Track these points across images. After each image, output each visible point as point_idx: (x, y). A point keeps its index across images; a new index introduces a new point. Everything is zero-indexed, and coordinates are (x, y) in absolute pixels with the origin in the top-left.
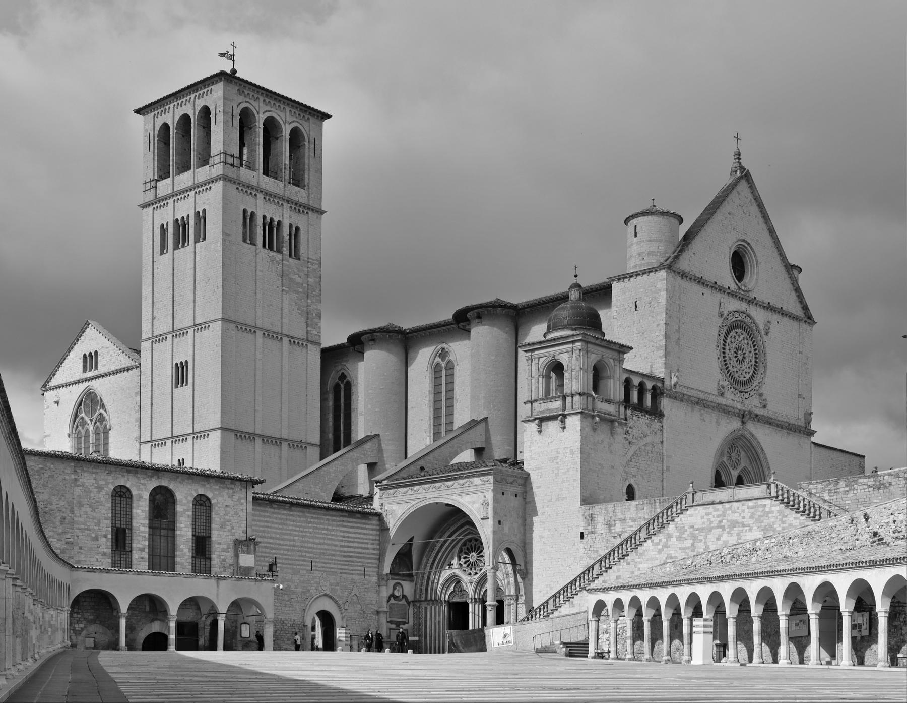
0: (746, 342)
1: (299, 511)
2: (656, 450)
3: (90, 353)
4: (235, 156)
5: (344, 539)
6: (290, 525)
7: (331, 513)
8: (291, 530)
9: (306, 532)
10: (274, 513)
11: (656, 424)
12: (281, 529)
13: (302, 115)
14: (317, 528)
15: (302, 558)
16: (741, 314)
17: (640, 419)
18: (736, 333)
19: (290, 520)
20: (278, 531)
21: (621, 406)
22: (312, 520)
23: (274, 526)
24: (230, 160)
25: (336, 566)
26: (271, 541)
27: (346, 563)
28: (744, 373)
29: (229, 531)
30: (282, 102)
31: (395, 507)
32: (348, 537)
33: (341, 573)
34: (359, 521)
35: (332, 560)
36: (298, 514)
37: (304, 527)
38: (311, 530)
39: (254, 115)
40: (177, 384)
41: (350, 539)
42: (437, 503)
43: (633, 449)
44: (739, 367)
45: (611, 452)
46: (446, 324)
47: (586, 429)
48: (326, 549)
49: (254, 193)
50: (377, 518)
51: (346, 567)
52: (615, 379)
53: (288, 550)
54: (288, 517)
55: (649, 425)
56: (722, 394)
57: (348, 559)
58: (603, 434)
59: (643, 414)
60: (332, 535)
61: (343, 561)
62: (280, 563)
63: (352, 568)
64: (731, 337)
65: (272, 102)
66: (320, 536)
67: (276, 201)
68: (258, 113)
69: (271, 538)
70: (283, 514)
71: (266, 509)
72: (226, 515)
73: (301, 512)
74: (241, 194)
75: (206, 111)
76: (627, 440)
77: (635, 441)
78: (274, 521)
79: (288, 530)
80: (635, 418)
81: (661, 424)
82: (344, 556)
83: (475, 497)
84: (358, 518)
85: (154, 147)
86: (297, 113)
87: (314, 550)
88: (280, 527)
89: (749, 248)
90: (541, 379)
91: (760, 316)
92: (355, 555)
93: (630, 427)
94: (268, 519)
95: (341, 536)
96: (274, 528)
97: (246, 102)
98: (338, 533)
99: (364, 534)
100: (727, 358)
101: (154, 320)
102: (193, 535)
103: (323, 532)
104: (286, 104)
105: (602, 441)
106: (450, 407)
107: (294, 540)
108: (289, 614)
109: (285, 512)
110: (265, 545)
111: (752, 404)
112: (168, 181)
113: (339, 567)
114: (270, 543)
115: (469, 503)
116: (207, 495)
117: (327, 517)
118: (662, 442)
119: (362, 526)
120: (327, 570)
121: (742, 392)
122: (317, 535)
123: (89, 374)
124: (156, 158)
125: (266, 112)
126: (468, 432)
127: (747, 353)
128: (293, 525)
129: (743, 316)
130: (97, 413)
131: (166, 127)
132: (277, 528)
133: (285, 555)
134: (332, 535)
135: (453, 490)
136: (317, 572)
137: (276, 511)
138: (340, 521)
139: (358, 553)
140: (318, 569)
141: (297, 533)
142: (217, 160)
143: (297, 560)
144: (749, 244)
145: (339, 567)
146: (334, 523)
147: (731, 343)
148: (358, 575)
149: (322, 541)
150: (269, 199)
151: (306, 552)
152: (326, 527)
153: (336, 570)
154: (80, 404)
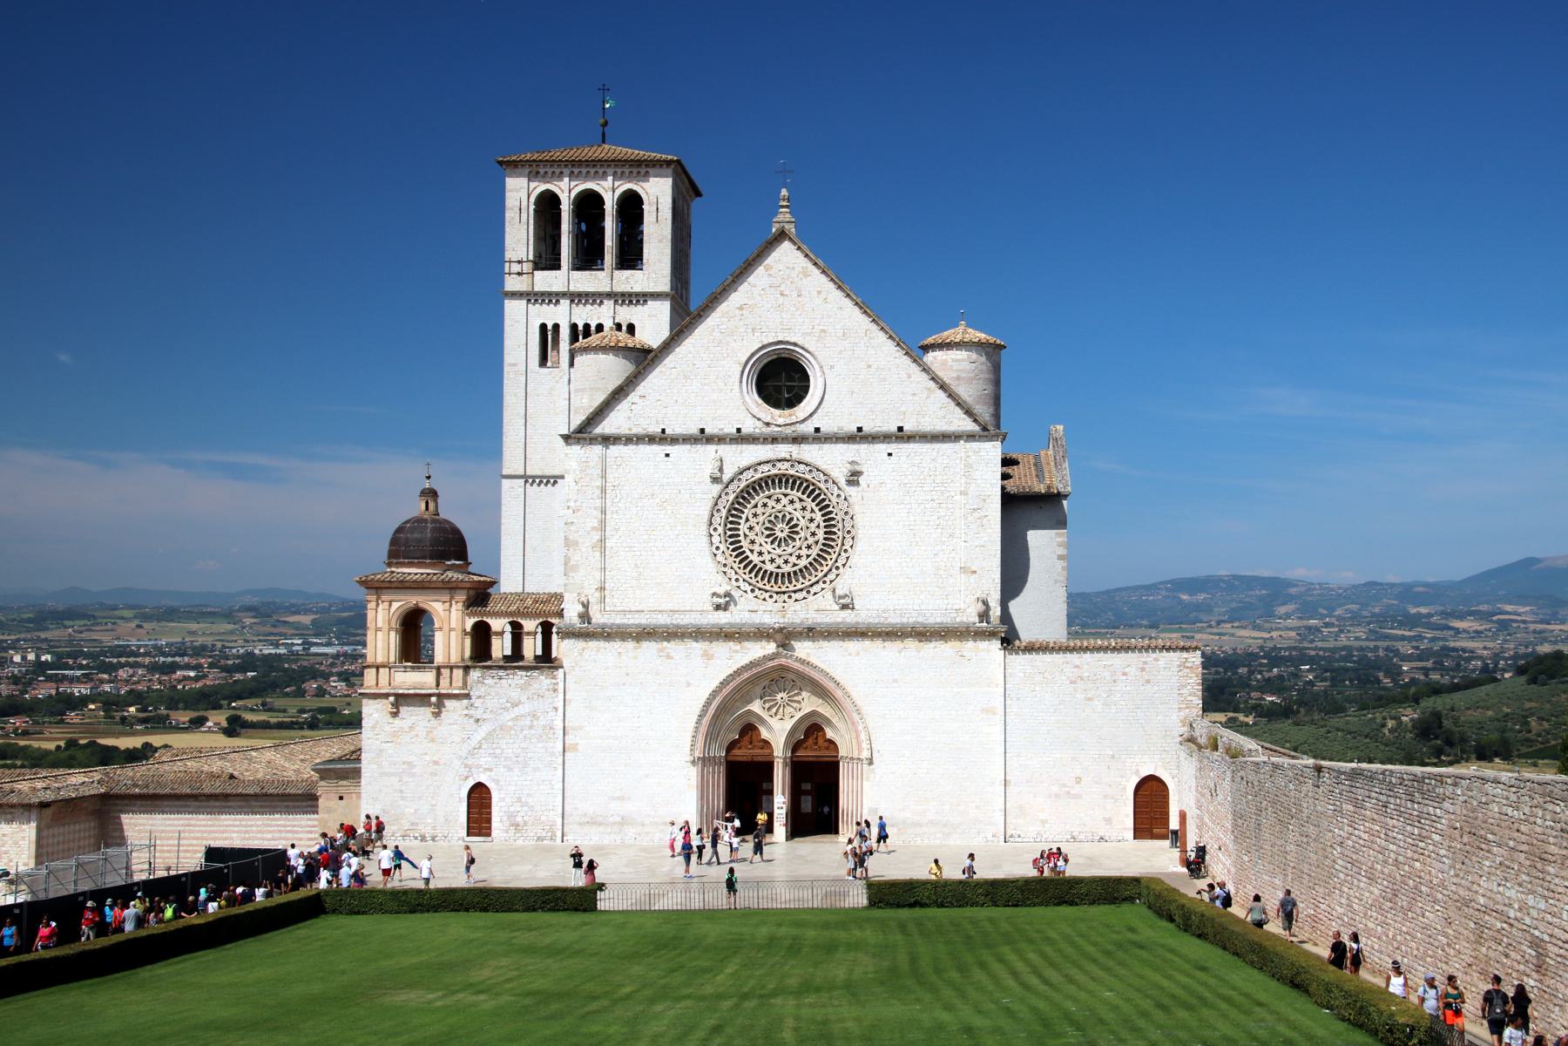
0: (798, 505)
2: (542, 721)
6: (225, 820)
8: (227, 826)
9: (252, 826)
10: (199, 807)
11: (542, 680)
12: (211, 826)
16: (779, 465)
17: (504, 681)
18: (769, 497)
20: (204, 829)
21: (455, 671)
23: (199, 823)
26: (195, 842)
28: (793, 559)
36: (239, 804)
43: (485, 729)
44: (779, 551)
45: (433, 740)
47: (376, 715)
52: (446, 628)
55: (523, 688)
56: (718, 607)
58: (415, 716)
59: (509, 672)
60: (295, 826)
64: (756, 506)
69: (197, 839)
76: (471, 717)
77: (490, 716)
79: (223, 826)
80: (489, 681)
81: (554, 681)
88: (210, 823)
89: (797, 349)
90: (393, 634)
91: (832, 460)
93: (480, 697)
96: (200, 826)
100: (745, 544)
105: (411, 728)
107: (232, 838)
109: (218, 804)
111: (816, 608)
117: (286, 804)
118: (556, 709)
121: (784, 593)
122: (269, 829)
127: (803, 523)
129: (787, 465)
132: (204, 826)
134: (295, 826)
137: (203, 804)
138: (308, 806)
141: (236, 829)
144: (795, 344)
147: (755, 515)
149: (277, 835)
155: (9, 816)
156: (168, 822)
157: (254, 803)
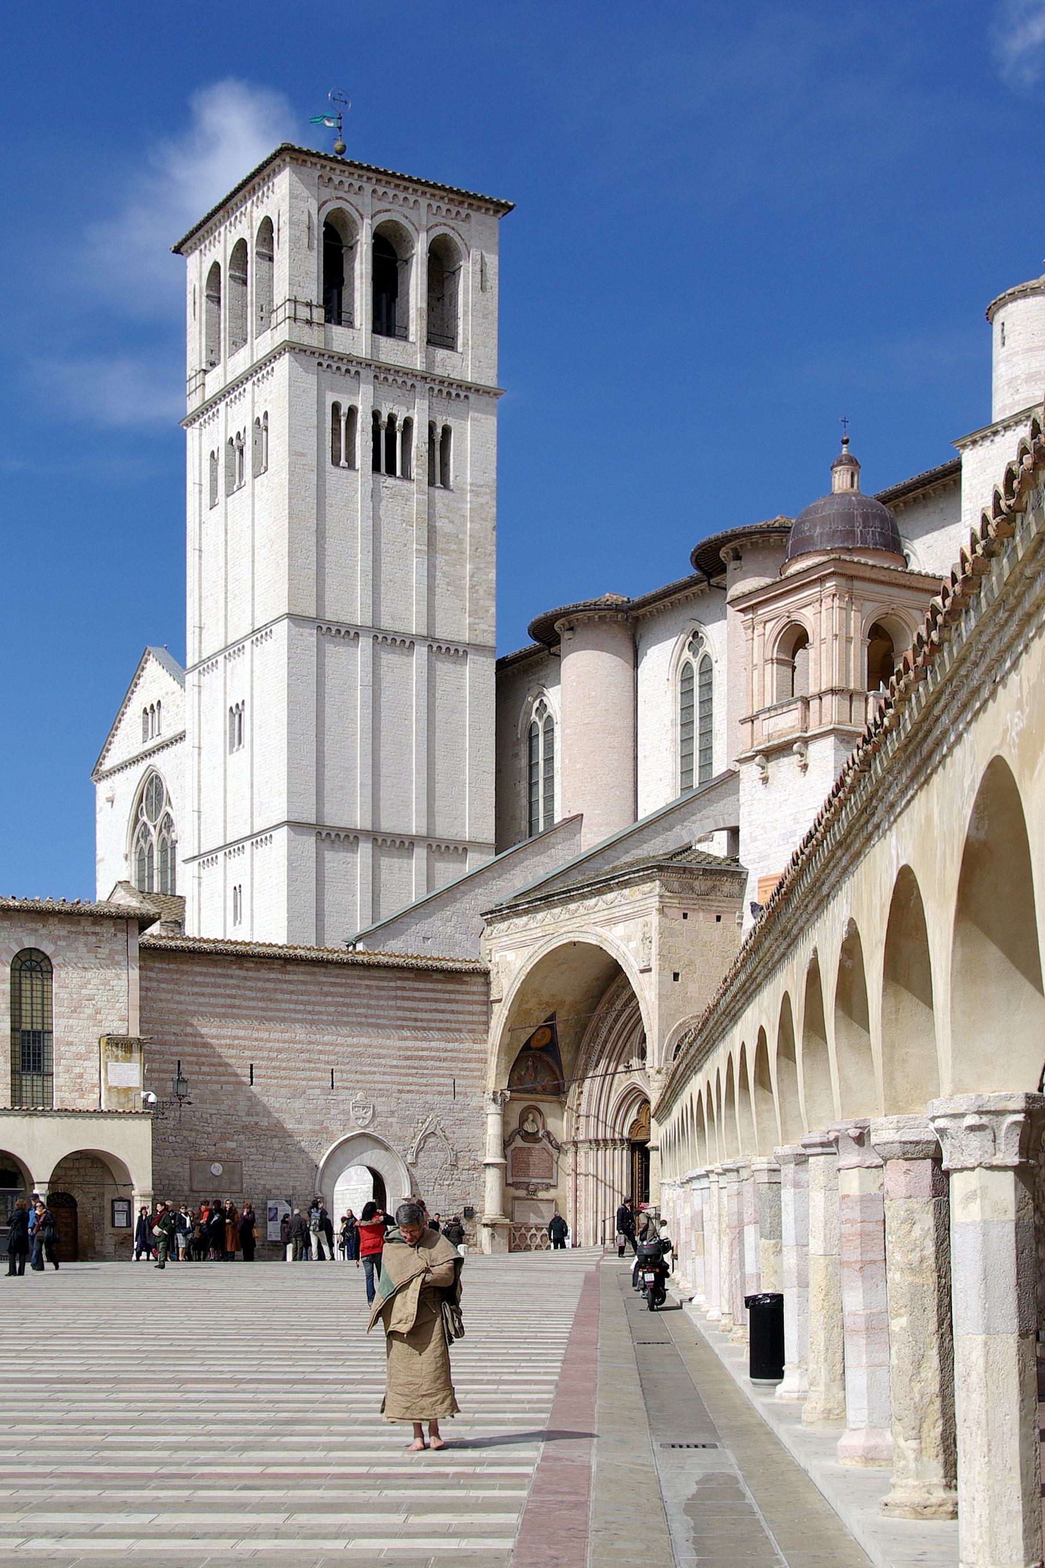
1: (302, 973)
3: (152, 706)
4: (314, 303)
5: (405, 1023)
6: (282, 1001)
7: (375, 973)
8: (286, 1011)
9: (320, 1013)
10: (245, 978)
12: (263, 1009)
13: (454, 210)
14: (344, 1005)
15: (312, 1065)
19: (283, 992)
20: (255, 1013)
22: (332, 989)
24: (303, 313)
25: (388, 1078)
27: (415, 1071)
29: (90, 1017)
30: (410, 190)
31: (510, 956)
32: (416, 1020)
33: (400, 1092)
34: (440, 986)
35: (380, 1065)
36: (302, 978)
37: (314, 1003)
38: (332, 1009)
39: (354, 222)
40: (232, 745)
41: (419, 1024)
42: (575, 944)
46: (693, 582)
48: (365, 1046)
49: (353, 370)
50: (483, 980)
51: (411, 1079)
53: (279, 1051)
54: (279, 986)
57: (416, 1063)
61: (403, 1067)
62: (259, 1077)
63: (424, 1081)
65: (391, 193)
66: (350, 1019)
67: (400, 380)
68: (362, 216)
70: (268, 980)
71: (229, 972)
72: (82, 987)
73: (309, 974)
74: (329, 374)
75: (267, 224)
78: (248, 993)
82: (407, 1058)
83: (631, 924)
84: (438, 981)
85: (201, 310)
86: (444, 207)
87: (337, 1049)
88: (262, 1004)
92: (433, 1054)
94: (234, 992)
95: (399, 1019)
97: (337, 198)
98: (392, 1013)
99: (452, 1012)
101: (204, 631)
102: (12, 1030)
103: (357, 1011)
104: (419, 193)
106: (707, 751)
108: (282, 1175)
109: (272, 976)
110: (228, 1041)
112: (218, 370)
113: (397, 1079)
114: (235, 1038)
115: (622, 938)
116: (42, 949)
117: (367, 982)
119: (447, 996)
120: (368, 1086)
122: (345, 1019)
123: (151, 744)
124: (204, 331)
125: (379, 212)
126: (708, 796)
128: (290, 1001)
130: (162, 813)
131: (216, 266)
132: (254, 1008)
133: (272, 1060)
134: (379, 1017)
135: (597, 915)
136: (346, 1091)
137: (251, 974)
138: (398, 988)
139: (438, 1050)
140: (346, 1084)
142: (281, 315)
143: (298, 1069)
145: (397, 1079)
146: (382, 993)
148: (440, 1093)
150: (386, 379)
151: (320, 1052)
152: (365, 1001)
153: (389, 1086)
154: (141, 801)
155: (93, 939)
156: (202, 1000)
157: (325, 979)
